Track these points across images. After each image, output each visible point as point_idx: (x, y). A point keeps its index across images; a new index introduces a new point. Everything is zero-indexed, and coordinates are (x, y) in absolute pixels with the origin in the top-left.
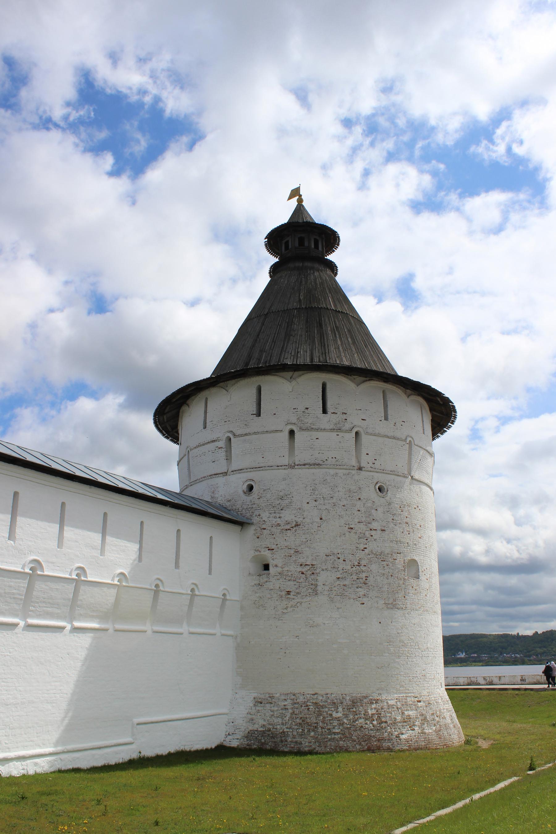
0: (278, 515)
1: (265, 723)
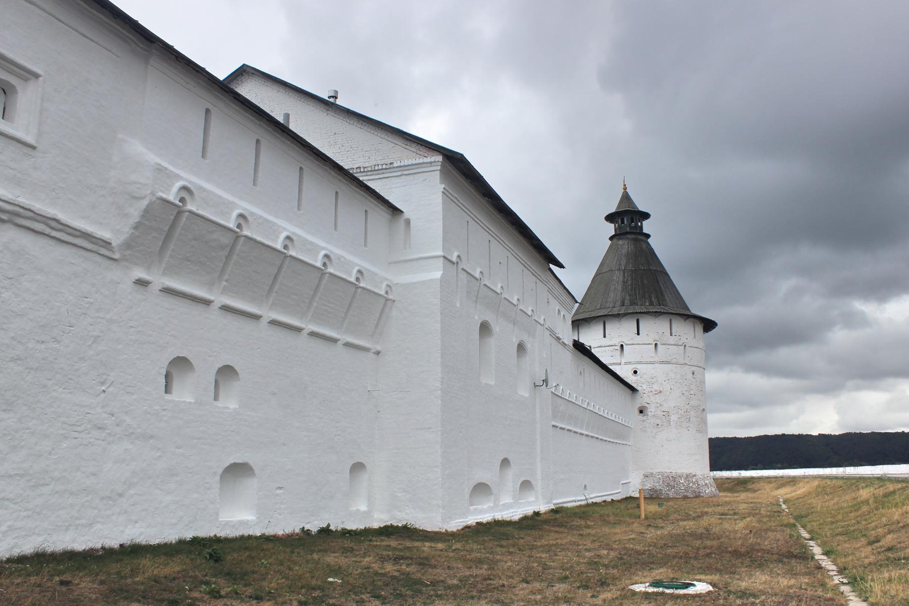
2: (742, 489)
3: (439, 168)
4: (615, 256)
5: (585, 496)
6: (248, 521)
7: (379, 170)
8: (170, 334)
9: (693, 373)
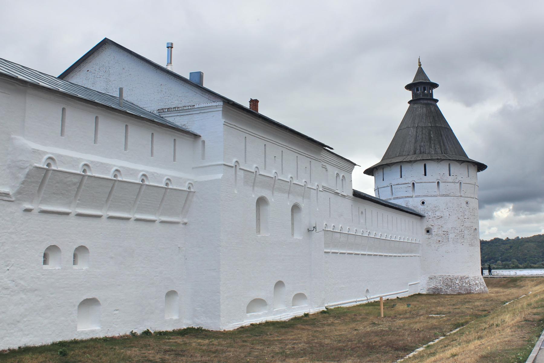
0: (434, 214)
1: (434, 285)
2: (513, 285)
3: (221, 109)
4: (411, 116)
5: (367, 297)
6: (96, 330)
7: (186, 109)
8: (46, 234)
9: (467, 203)
